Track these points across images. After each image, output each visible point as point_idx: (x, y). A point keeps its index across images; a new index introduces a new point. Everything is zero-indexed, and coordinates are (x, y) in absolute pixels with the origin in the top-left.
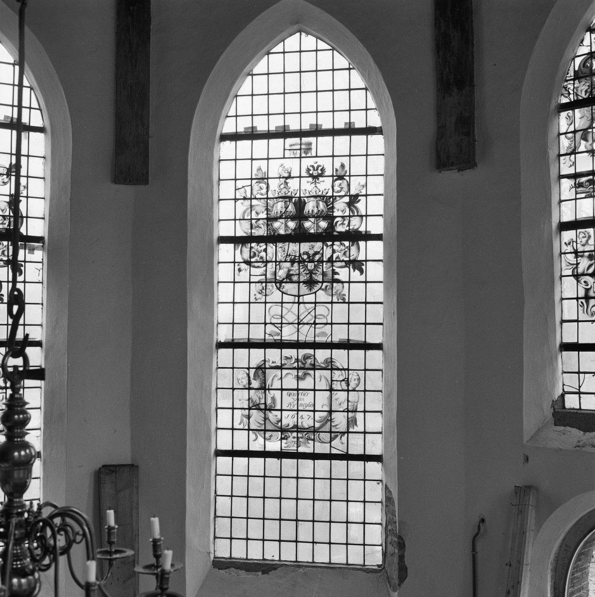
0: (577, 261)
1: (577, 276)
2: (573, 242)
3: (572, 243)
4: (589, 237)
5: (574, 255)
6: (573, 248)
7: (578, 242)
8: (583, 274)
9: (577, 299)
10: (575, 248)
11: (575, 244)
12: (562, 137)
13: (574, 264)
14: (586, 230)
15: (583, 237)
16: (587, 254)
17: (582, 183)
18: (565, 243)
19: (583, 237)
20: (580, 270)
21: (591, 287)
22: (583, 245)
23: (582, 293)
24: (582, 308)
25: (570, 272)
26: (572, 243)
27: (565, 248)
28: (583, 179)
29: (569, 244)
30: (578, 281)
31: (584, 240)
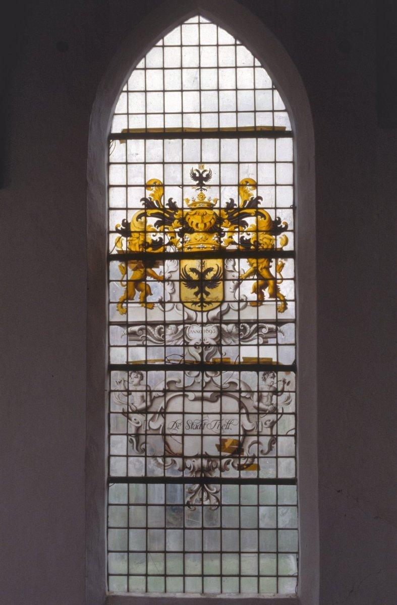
2: (124, 381)
3: (122, 382)
4: (142, 379)
6: (125, 387)
10: (127, 388)
21: (141, 426)
22: (135, 385)
24: (132, 445)
26: (122, 382)
29: (120, 382)
30: (129, 418)
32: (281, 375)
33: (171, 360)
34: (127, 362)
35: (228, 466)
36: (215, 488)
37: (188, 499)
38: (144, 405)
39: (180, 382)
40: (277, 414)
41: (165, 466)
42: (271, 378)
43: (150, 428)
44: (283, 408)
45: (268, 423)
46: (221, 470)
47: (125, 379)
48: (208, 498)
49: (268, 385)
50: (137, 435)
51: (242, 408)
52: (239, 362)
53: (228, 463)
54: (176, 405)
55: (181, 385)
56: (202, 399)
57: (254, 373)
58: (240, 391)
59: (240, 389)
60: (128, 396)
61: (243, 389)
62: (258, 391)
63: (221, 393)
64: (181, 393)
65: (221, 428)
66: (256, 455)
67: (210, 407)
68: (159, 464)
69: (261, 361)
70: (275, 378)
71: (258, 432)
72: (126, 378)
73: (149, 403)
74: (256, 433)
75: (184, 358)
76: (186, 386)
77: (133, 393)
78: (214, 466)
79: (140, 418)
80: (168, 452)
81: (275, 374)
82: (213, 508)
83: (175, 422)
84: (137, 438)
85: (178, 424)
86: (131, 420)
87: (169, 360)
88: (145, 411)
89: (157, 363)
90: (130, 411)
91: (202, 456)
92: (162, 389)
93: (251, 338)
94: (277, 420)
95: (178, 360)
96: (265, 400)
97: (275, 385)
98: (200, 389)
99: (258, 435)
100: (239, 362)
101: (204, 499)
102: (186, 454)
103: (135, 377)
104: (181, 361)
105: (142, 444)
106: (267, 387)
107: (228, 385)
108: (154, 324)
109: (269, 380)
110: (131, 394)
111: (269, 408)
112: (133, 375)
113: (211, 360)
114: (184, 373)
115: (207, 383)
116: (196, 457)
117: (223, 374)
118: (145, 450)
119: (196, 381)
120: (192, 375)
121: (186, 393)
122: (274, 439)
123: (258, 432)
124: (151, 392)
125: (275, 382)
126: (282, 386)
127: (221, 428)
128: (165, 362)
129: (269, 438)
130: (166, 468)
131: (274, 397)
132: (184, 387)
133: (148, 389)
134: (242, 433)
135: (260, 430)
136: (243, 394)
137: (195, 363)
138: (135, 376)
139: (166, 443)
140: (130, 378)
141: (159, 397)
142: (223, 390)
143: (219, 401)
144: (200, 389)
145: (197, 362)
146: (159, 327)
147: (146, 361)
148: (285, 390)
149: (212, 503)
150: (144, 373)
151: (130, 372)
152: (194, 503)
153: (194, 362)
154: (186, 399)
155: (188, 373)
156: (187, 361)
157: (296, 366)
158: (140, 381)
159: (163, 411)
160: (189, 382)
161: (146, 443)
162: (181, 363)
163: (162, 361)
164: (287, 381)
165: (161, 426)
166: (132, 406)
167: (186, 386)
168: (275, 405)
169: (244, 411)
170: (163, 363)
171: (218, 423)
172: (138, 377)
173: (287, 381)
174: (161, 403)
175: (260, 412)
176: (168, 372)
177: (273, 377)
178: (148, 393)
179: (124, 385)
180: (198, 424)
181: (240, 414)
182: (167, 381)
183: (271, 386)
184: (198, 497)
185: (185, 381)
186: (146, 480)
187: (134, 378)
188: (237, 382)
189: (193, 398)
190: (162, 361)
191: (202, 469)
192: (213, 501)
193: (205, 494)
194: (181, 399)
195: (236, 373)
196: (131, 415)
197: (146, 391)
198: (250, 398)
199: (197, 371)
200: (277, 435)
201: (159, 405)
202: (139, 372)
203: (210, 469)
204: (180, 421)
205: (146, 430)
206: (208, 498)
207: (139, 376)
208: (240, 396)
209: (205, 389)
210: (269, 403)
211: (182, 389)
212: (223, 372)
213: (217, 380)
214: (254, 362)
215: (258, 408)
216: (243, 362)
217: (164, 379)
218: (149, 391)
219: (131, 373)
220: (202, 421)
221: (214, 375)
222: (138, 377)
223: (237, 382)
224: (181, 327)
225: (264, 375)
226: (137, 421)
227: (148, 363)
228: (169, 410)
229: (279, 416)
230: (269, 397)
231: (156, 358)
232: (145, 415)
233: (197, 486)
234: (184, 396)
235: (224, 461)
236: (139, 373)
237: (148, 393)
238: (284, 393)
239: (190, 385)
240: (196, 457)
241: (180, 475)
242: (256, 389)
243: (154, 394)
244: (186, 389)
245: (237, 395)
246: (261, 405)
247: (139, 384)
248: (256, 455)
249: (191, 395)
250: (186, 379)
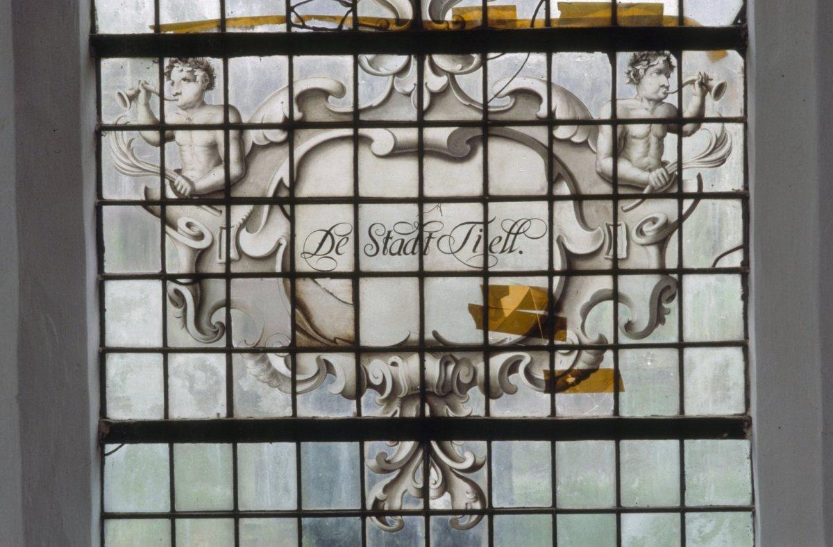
2: (148, 92)
3: (142, 95)
4: (209, 85)
10: (158, 117)
11: (156, 99)
22: (186, 107)
24: (179, 311)
26: (142, 95)
29: (133, 98)
30: (166, 222)
32: (695, 61)
33: (310, 17)
34: (157, 26)
35: (512, 379)
36: (467, 452)
37: (375, 492)
38: (218, 176)
39: (342, 92)
40: (681, 196)
41: (294, 382)
42: (660, 72)
43: (241, 253)
44: (699, 177)
45: (650, 230)
46: (489, 392)
47: (151, 87)
48: (446, 486)
49: (649, 100)
50: (197, 278)
51: (560, 178)
52: (548, 19)
53: (512, 367)
54: (329, 172)
55: (344, 105)
56: (420, 151)
57: (600, 58)
58: (550, 122)
59: (551, 113)
60: (161, 144)
61: (560, 114)
62: (614, 121)
63: (487, 128)
64: (348, 132)
65: (487, 249)
66: (611, 341)
67: (446, 177)
68: (275, 374)
69: (621, 14)
70: (674, 74)
71: (615, 260)
72: (154, 84)
73: (235, 170)
74: (607, 265)
75: (354, 10)
76: (362, 105)
77: (180, 135)
78: (465, 380)
79: (206, 218)
80: (304, 332)
81: (674, 61)
82: (466, 520)
83: (328, 232)
84: (198, 288)
85: (337, 240)
86: (175, 227)
87: (301, 18)
88: (222, 197)
89: (259, 29)
90: (171, 195)
91: (422, 347)
92: (278, 118)
94: (682, 218)
95: (333, 18)
96: (637, 150)
97: (672, 99)
98: (412, 115)
99: (616, 271)
100: (548, 19)
101: (432, 493)
102: (367, 340)
103: (184, 79)
104: (343, 20)
106: (646, 104)
107: (508, 102)
109: (652, 82)
110: (172, 138)
111: (654, 178)
112: (179, 71)
113: (449, 16)
114: (357, 63)
115: (434, 95)
116: (403, 348)
117: (490, 63)
118: (227, 328)
119: (397, 88)
120: (383, 71)
121: (362, 131)
122: (671, 283)
123: (615, 260)
124: (242, 128)
125: (674, 86)
126: (696, 101)
127: (487, 249)
128: (290, 25)
129: (653, 281)
130: (299, 388)
131: (671, 139)
132: (357, 111)
133: (232, 119)
134: (558, 265)
135: (622, 253)
136: (562, 132)
137: (393, 27)
138: (184, 74)
139: (296, 303)
140: (167, 84)
141: (272, 145)
142: (491, 117)
143: (480, 150)
144: (412, 115)
145: (399, 21)
147: (223, 22)
148: (708, 114)
149: (461, 505)
150: (216, 63)
151: (167, 62)
152: (397, 504)
153: (388, 21)
154: (364, 152)
155: (370, 63)
156: (366, 19)
157: (746, 28)
158: (202, 91)
159: (284, 194)
160: (372, 92)
161: (228, 304)
162: (345, 28)
163: (279, 20)
164: (714, 84)
165: (279, 245)
166: (179, 180)
167: (362, 105)
168: (672, 168)
169: (564, 189)
170: (282, 28)
171: (477, 231)
172: (195, 80)
173: (714, 84)
174: (276, 167)
175: (620, 192)
176: (299, 60)
177: (667, 70)
178: (232, 133)
179: (147, 105)
180: (406, 238)
181: (551, 198)
182: (297, 91)
183: (659, 102)
184: (410, 484)
185: (361, 88)
186: (231, 431)
187: (182, 80)
188: (542, 90)
189: (388, 148)
190: (279, 20)
191: (423, 391)
192: (464, 496)
193: (435, 475)
194: (346, 150)
195: (538, 59)
196: (173, 210)
197: (225, 126)
198: (584, 144)
199: (401, 53)
200: (682, 271)
201: (270, 173)
202: (199, 59)
203: (449, 390)
204: (347, 228)
205: (229, 261)
206: (446, 486)
207: (199, 74)
208: (552, 138)
209: (430, 117)
210: (653, 162)
211: (349, 119)
212: (491, 55)
213: (471, 82)
214: (597, 19)
215: (614, 180)
216: (561, 20)
217: (286, 83)
218: (234, 126)
219: (171, 67)
220: (421, 225)
221: (457, 67)
222: (195, 80)
223: (542, 90)
225: (634, 63)
226: (195, 231)
227: (230, 30)
228: (305, 190)
229: (687, 204)
230: (653, 140)
231: (257, 13)
232: (223, 208)
233: (408, 446)
234: (357, 141)
235: (498, 361)
236: (198, 66)
237: (232, 133)
238: (704, 125)
239: (375, 102)
240: (403, 348)
241: (347, 411)
242: (606, 114)
243: (253, 136)
244: (363, 117)
245: (540, 134)
246: (626, 169)
247: (200, 102)
248: (611, 341)
249: (382, 139)
250: (361, 82)
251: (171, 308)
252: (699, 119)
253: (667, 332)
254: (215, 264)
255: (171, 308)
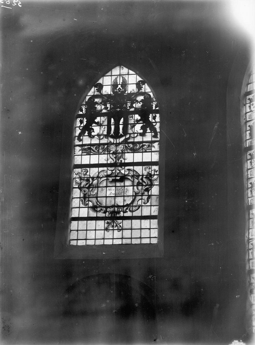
0: (81, 181)
1: (80, 188)
4: (87, 171)
5: (79, 179)
6: (79, 176)
7: (82, 173)
8: (83, 187)
9: (80, 198)
11: (80, 174)
12: (77, 128)
13: (79, 183)
14: (86, 168)
15: (84, 171)
16: (85, 179)
17: (85, 149)
18: (76, 174)
19: (84, 171)
20: (82, 186)
23: (82, 195)
25: (77, 186)
27: (75, 176)
28: (86, 147)
29: (78, 174)
31: (85, 173)
64: (106, 178)
66: (141, 205)
84: (85, 198)
93: (137, 151)
105: (87, 201)
108: (93, 145)
116: (113, 206)
122: (149, 197)
129: (147, 197)
134: (134, 194)
146: (96, 146)
150: (88, 169)
154: (108, 181)
224: (106, 146)
242: (142, 174)
248: (141, 205)
249: (111, 179)
251: (81, 202)
252: (154, 175)
253: (149, 204)
254: (87, 196)
255: (81, 202)
